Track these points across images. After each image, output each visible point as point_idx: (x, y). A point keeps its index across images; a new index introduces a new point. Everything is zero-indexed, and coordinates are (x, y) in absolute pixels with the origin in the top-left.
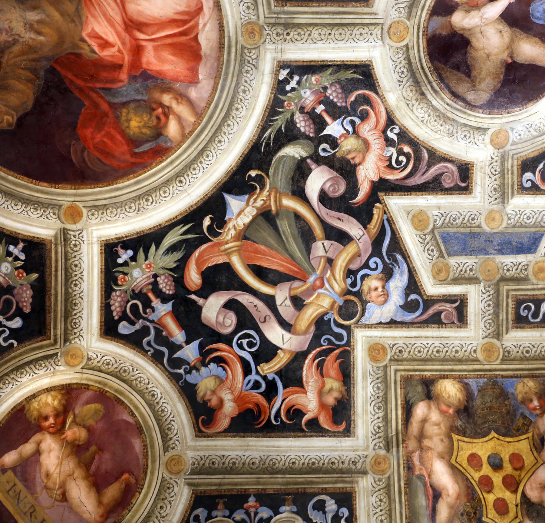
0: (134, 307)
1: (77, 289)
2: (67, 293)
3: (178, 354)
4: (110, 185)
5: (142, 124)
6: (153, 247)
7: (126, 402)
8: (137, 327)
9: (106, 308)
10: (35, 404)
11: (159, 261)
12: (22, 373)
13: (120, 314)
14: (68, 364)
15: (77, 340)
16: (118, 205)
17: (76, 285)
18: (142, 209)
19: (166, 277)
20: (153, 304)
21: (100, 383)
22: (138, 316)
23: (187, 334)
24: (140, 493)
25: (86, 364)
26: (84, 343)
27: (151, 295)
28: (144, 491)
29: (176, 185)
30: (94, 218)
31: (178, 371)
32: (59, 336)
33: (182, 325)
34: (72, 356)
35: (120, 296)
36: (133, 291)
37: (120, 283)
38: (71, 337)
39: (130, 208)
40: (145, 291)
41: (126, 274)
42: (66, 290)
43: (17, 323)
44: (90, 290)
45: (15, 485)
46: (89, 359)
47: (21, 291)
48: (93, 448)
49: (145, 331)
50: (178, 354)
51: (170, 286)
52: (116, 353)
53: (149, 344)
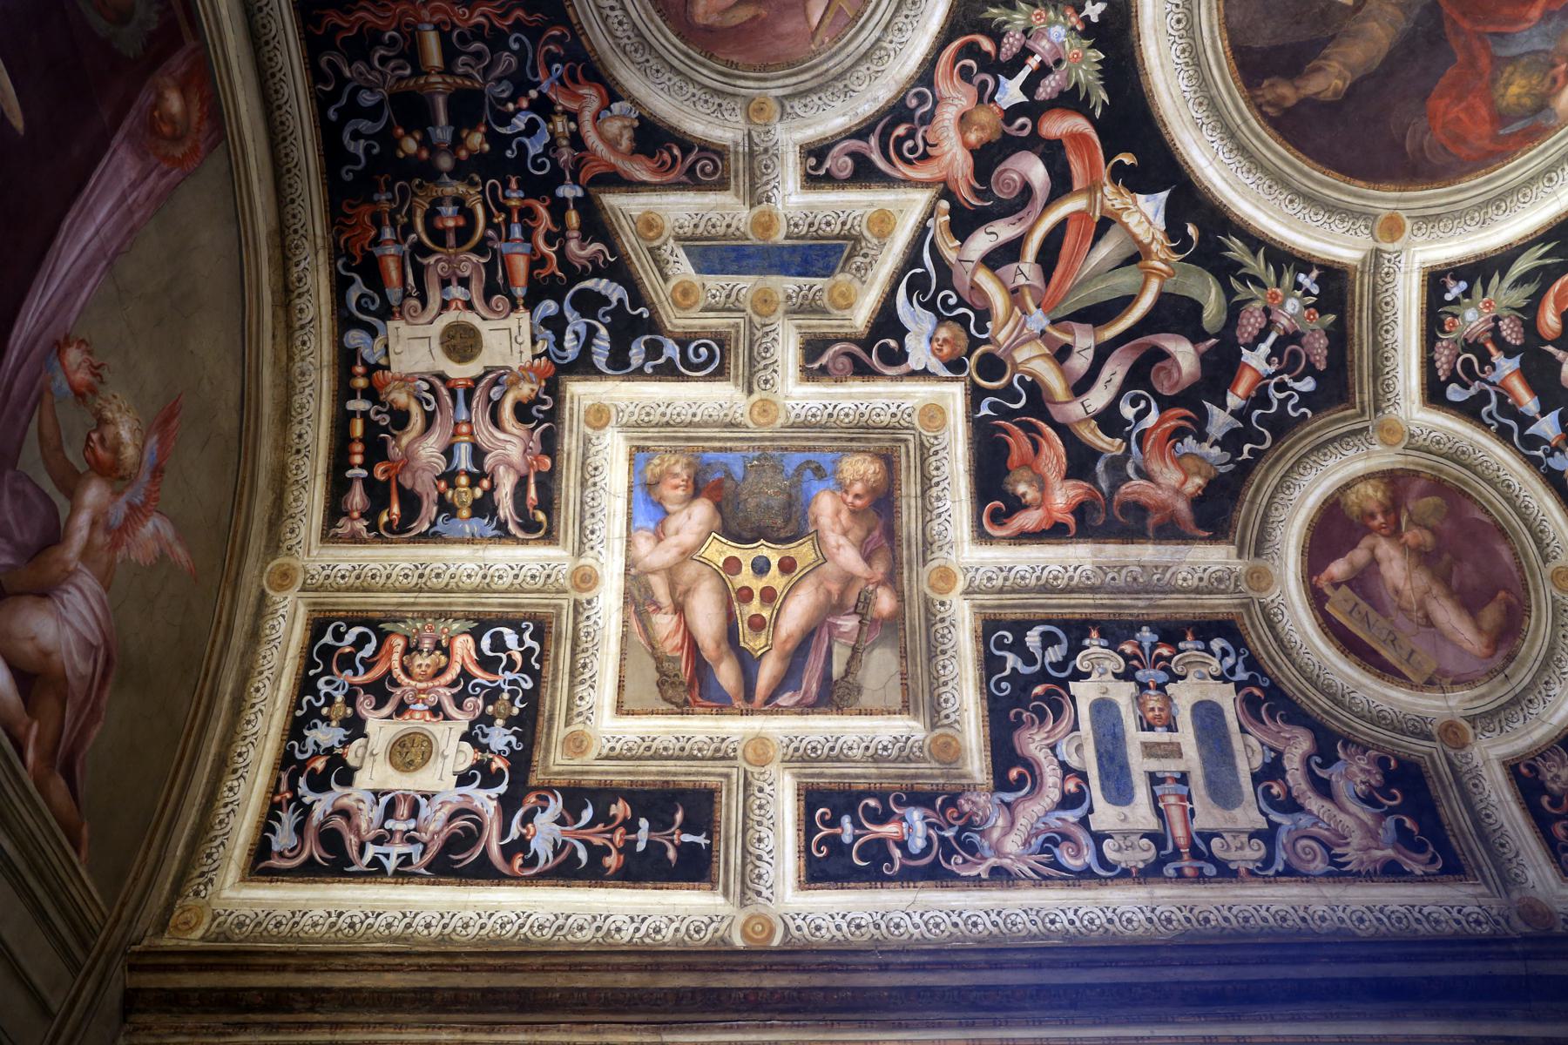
0: (1467, 364)
1: (1389, 336)
2: (1375, 343)
3: (1532, 430)
4: (1450, 185)
5: (1524, 90)
6: (1496, 278)
7: (1473, 494)
8: (1473, 391)
9: (1429, 365)
10: (1352, 497)
11: (1502, 297)
12: (1325, 455)
13: (1448, 373)
14: (1384, 442)
15: (1391, 409)
16: (1456, 214)
17: (1387, 331)
18: (1488, 221)
19: (1512, 321)
20: (1494, 359)
21: (1432, 468)
22: (1473, 376)
23: (1541, 402)
24: (1529, 617)
25: (1409, 443)
26: (1401, 414)
27: (1490, 347)
28: (1533, 614)
29: (1542, 185)
30: (1420, 233)
31: (1536, 453)
32: (1366, 403)
33: (1534, 389)
34: (1388, 431)
35: (1447, 347)
36: (1466, 340)
37: (1447, 328)
38: (1384, 405)
39: (1472, 219)
40: (1481, 340)
41: (1456, 316)
42: (1375, 338)
43: (1308, 385)
44: (1407, 338)
45: (1356, 604)
46: (1412, 436)
47: (1311, 339)
48: (1447, 557)
49: (1483, 397)
50: (1532, 430)
51: (1517, 333)
52: (1447, 428)
53: (1490, 415)
